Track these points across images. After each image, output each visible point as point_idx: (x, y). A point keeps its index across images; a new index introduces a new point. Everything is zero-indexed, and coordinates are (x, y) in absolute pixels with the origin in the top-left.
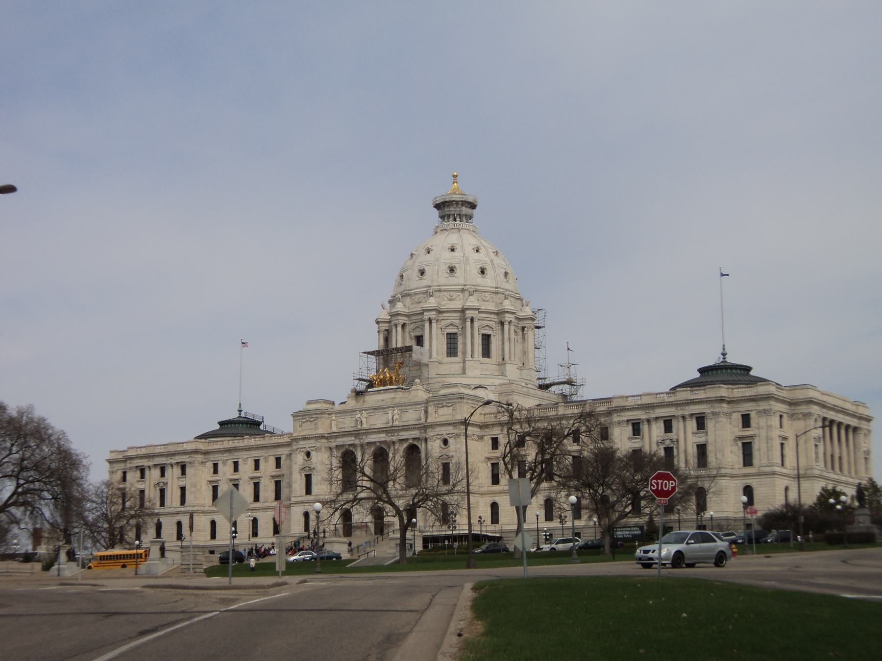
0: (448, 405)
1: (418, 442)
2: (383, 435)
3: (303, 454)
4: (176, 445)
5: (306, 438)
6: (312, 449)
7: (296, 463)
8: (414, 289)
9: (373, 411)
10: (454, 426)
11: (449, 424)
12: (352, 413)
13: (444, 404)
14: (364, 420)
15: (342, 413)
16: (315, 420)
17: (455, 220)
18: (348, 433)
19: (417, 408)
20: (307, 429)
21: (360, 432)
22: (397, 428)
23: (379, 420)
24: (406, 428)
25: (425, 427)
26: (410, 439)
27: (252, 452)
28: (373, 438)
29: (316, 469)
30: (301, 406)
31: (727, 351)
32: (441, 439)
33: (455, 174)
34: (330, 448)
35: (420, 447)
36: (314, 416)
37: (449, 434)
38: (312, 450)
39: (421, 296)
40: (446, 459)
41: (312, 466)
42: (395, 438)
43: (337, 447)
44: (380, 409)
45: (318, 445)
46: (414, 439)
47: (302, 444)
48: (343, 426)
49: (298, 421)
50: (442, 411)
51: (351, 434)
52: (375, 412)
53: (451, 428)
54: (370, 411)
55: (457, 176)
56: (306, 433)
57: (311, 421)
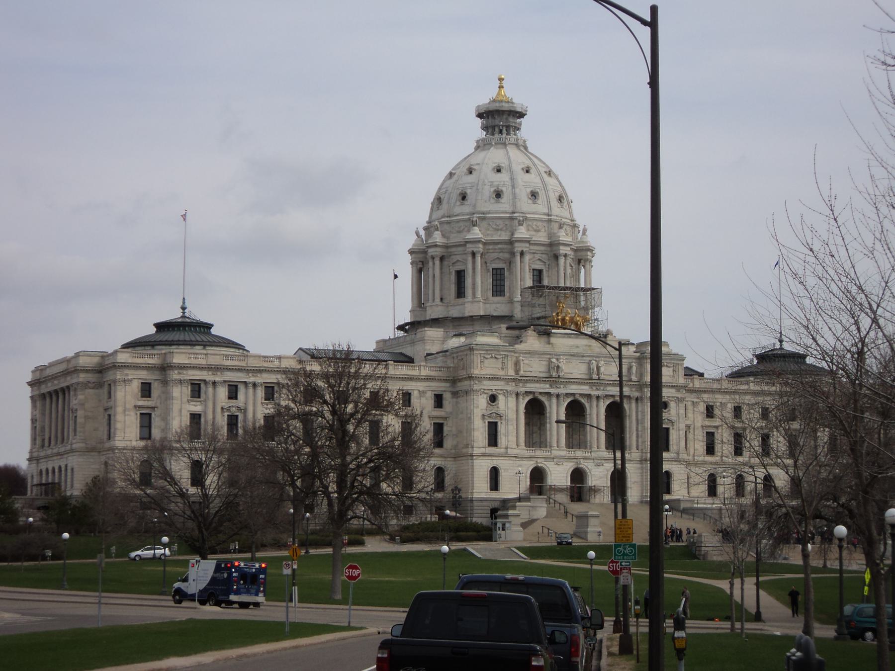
0: (669, 365)
2: (587, 387)
3: (485, 396)
4: (262, 358)
5: (494, 378)
6: (499, 392)
7: (478, 407)
9: (570, 357)
10: (677, 389)
11: (672, 386)
12: (542, 356)
15: (529, 354)
17: (501, 132)
28: (574, 389)
33: (503, 77)
34: (517, 393)
36: (502, 353)
38: (499, 394)
41: (501, 412)
43: (527, 393)
44: (578, 356)
45: (509, 388)
47: (487, 384)
53: (673, 391)
55: (503, 79)
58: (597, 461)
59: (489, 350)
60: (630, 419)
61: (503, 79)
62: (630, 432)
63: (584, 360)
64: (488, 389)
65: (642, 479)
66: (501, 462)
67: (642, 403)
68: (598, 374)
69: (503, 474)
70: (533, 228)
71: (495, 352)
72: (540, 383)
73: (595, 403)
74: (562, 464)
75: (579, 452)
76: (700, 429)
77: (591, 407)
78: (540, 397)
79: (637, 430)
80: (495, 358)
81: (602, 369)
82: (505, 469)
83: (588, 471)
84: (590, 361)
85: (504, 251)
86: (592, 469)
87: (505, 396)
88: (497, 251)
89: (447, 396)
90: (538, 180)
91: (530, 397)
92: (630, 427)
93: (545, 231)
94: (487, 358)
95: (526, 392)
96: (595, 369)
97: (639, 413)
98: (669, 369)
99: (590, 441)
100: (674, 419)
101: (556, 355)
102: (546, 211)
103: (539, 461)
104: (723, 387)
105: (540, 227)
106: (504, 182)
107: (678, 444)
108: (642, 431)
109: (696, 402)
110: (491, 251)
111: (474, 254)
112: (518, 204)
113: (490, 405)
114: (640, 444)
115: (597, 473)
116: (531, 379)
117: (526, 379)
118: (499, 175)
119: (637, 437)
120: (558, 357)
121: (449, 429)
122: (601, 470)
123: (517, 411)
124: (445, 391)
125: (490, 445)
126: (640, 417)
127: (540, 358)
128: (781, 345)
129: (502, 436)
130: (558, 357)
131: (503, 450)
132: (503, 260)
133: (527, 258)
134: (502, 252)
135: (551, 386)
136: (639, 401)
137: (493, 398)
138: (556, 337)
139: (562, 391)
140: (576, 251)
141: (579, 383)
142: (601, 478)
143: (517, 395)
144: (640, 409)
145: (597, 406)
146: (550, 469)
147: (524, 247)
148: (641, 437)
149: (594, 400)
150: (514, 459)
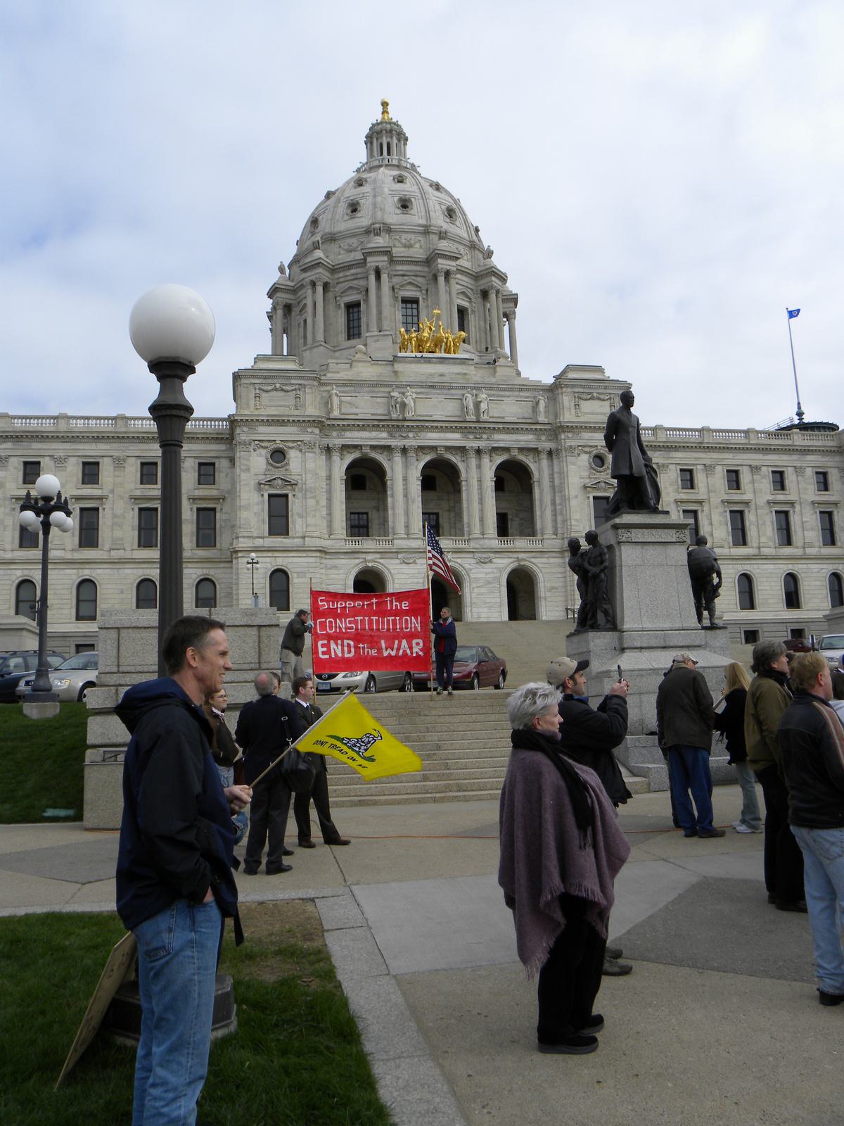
0: (602, 397)
2: (457, 436)
6: (291, 444)
7: (248, 470)
8: (396, 225)
9: (427, 390)
13: (595, 395)
14: (409, 401)
15: (351, 385)
16: (295, 390)
18: (376, 423)
19: (522, 397)
20: (274, 404)
22: (492, 426)
23: (441, 408)
24: (510, 428)
25: (556, 430)
27: (80, 446)
28: (432, 438)
29: (300, 486)
30: (248, 363)
31: (803, 409)
35: (533, 467)
36: (293, 382)
38: (289, 448)
39: (412, 236)
40: (605, 490)
41: (293, 478)
42: (481, 444)
43: (345, 448)
45: (307, 438)
46: (521, 449)
47: (265, 432)
48: (355, 411)
49: (251, 387)
50: (587, 406)
51: (383, 426)
52: (427, 394)
54: (419, 390)
56: (273, 411)
57: (287, 391)
58: (480, 555)
59: (270, 377)
60: (539, 486)
61: (387, 104)
62: (541, 506)
63: (452, 395)
64: (269, 441)
65: (565, 582)
66: (290, 560)
67: (559, 458)
69: (296, 580)
70: (401, 243)
71: (280, 381)
72: (370, 431)
73: (473, 462)
74: (414, 562)
75: (447, 542)
77: (467, 468)
78: (375, 455)
79: (554, 503)
80: (283, 390)
81: (483, 406)
82: (298, 573)
83: (464, 573)
84: (463, 395)
85: (359, 276)
86: (471, 569)
88: (349, 278)
89: (222, 465)
90: (415, 188)
91: (356, 455)
92: (541, 501)
93: (421, 247)
94: (267, 391)
95: (343, 445)
96: (471, 406)
97: (556, 475)
98: (603, 403)
99: (468, 523)
101: (397, 387)
102: (423, 222)
103: (369, 557)
104: (706, 441)
105: (412, 242)
106: (364, 193)
108: (561, 504)
109: (663, 465)
110: (342, 280)
111: (313, 284)
112: (379, 214)
113: (272, 465)
114: (559, 525)
115: (478, 576)
118: (361, 188)
119: (555, 515)
120: (402, 390)
121: (224, 517)
122: (491, 570)
123: (329, 478)
124: (217, 457)
125: (272, 532)
126: (557, 482)
127: (373, 392)
128: (801, 419)
129: (296, 517)
130: (402, 390)
131: (298, 541)
132: (358, 289)
133: (384, 277)
134: (357, 279)
135: (391, 436)
136: (554, 457)
137: (278, 455)
138: (405, 362)
139: (415, 443)
140: (476, 277)
141: (442, 429)
142: (490, 583)
143: (328, 450)
144: (556, 469)
145: (479, 467)
146: (392, 571)
147: (381, 261)
148: (561, 514)
149: (472, 454)
150: (318, 554)
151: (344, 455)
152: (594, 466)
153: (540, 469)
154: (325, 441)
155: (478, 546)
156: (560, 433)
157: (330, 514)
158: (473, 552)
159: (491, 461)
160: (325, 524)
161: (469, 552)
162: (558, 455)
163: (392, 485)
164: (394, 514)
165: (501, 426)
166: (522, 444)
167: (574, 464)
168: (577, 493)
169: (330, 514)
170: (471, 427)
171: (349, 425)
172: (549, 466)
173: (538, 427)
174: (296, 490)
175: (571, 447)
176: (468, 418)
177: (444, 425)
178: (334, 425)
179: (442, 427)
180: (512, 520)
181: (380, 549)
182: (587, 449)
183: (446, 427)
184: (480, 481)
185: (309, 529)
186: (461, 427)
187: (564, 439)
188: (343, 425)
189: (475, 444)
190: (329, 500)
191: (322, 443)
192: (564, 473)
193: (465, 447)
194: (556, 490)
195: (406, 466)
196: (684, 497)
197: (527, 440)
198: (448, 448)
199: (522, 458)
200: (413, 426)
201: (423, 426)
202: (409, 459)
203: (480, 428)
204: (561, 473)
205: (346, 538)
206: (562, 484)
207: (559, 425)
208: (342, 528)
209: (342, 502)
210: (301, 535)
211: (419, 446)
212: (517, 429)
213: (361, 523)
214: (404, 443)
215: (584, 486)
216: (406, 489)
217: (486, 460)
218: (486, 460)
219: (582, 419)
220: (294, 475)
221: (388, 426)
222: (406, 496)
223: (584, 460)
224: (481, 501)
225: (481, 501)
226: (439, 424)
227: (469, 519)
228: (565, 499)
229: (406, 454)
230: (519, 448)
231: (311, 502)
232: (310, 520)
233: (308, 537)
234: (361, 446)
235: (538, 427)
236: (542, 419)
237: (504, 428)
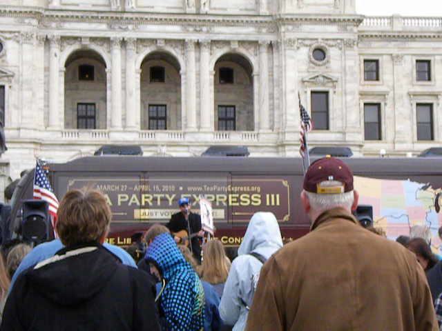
1: (247, 49)
2: (177, 28)
6: (8, 35)
18: (95, 15)
21: (125, 16)
22: (211, 18)
25: (276, 23)
26: (234, 41)
29: (16, 77)
32: (314, 46)
35: (253, 60)
37: (327, 40)
38: (6, 38)
40: (324, 85)
42: (201, 37)
43: (64, 39)
46: (241, 42)
51: (102, 18)
53: (334, 28)
68: (198, 8)
72: (90, 22)
73: (192, 54)
76: (406, 99)
77: (187, 62)
79: (272, 97)
87: (18, 42)
91: (76, 46)
92: (259, 95)
97: (275, 69)
99: (186, 117)
100: (335, 75)
107: (344, 118)
108: (278, 99)
109: (398, 56)
114: (276, 120)
116: (70, 14)
117: (60, 14)
119: (272, 108)
123: (47, 69)
126: (275, 76)
135: (111, 28)
139: (135, 35)
143: (47, 41)
144: (276, 63)
145: (198, 60)
148: (279, 108)
149: (191, 47)
150: (32, 146)
151: (64, 47)
152: (313, 59)
153: (259, 62)
154: (43, 33)
155: (193, 140)
156: (280, 25)
157: (47, 106)
158: (188, 146)
159: (211, 54)
160: (42, 115)
161: (184, 146)
162: (278, 48)
163: (111, 77)
164: (112, 107)
165: (221, 19)
166: (242, 38)
167: (292, 57)
168: (294, 88)
169: (47, 106)
170: (190, 20)
171: (67, 17)
172: (269, 59)
173: (259, 19)
174: (13, 81)
175: (290, 40)
176: (188, 10)
177: (163, 17)
178: (52, 16)
179: (161, 19)
180: (240, 113)
181: (96, 141)
182: (307, 42)
183: (166, 19)
184: (199, 74)
185: (24, 121)
186: (180, 20)
187: (284, 32)
188: (62, 16)
189: (195, 37)
190: (47, 91)
191: (41, 34)
192: (281, 67)
193: (184, 40)
194: (275, 84)
195: (125, 59)
196: (418, 89)
197: (247, 32)
198: (167, 41)
199: (242, 51)
200: (132, 19)
201: (142, 19)
202: (129, 51)
203: (200, 21)
204: (280, 67)
205: (64, 130)
206: (280, 77)
207: (278, 17)
208: (60, 120)
209: (60, 95)
210: (14, 126)
211: (138, 39)
212: (238, 21)
213: (89, 114)
214: (124, 36)
215: (302, 79)
216: (125, 82)
217: (205, 53)
218: (205, 53)
219: (305, 10)
220: (11, 66)
221: (107, 17)
222: (124, 88)
223: (305, 53)
224: (199, 95)
225: (199, 95)
226: (159, 17)
227: (186, 114)
228: (282, 94)
229: (125, 47)
230: (239, 42)
231: (27, 94)
232: (26, 112)
233: (23, 128)
234: (81, 38)
235: (259, 19)
236: (264, 10)
237: (223, 21)
